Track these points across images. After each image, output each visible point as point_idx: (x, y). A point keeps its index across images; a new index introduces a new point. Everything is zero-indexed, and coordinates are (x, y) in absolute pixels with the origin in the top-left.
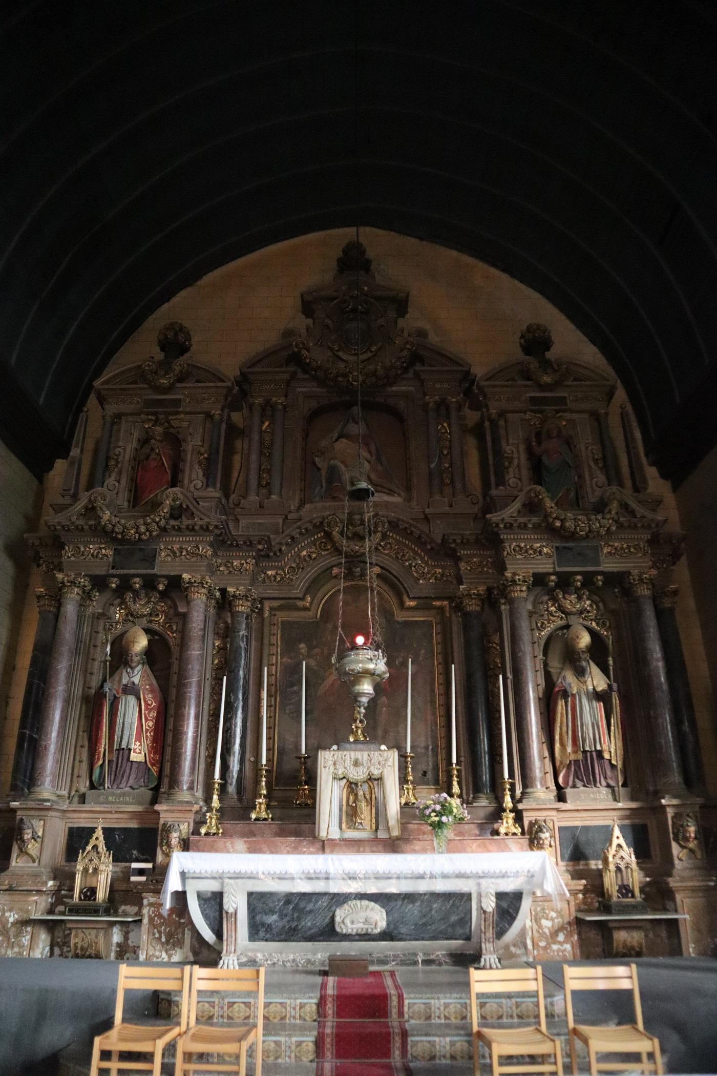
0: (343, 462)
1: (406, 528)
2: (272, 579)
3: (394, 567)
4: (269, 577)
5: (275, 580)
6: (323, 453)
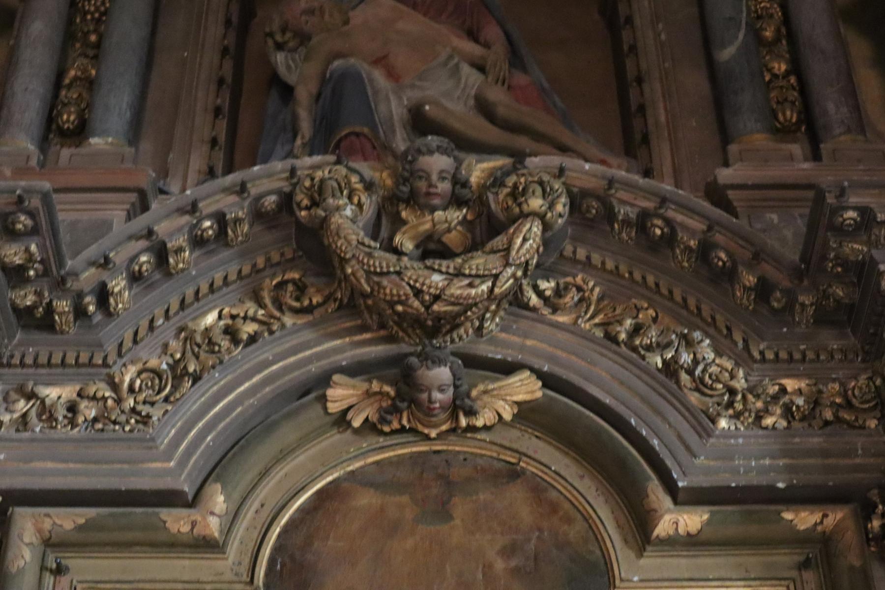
0: (380, 61)
1: (645, 215)
2: (61, 413)
3: (604, 377)
4: (47, 413)
5: (73, 423)
6: (304, 38)
